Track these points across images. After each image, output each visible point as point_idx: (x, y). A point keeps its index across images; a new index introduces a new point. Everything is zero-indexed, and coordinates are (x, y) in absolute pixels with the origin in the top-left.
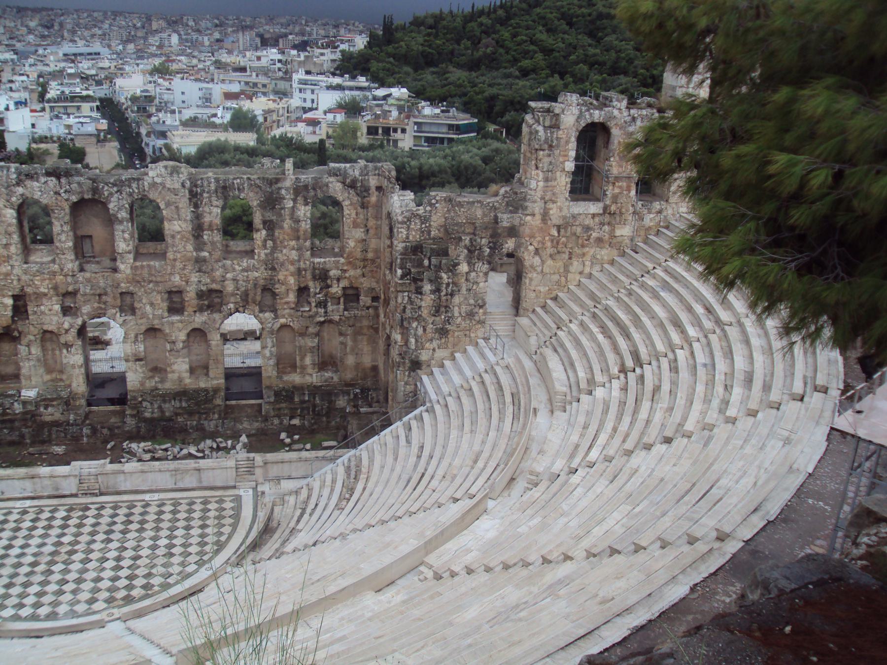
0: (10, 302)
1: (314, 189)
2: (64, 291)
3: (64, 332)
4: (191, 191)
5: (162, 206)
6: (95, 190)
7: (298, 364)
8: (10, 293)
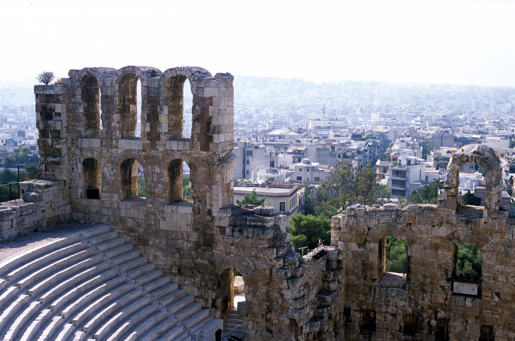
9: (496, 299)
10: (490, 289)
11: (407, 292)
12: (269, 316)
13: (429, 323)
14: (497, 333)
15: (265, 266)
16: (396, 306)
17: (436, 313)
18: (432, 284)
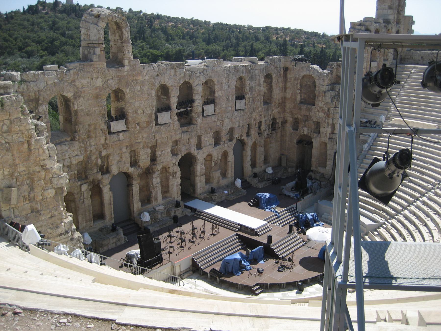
0: (149, 151)
1: (265, 70)
2: (175, 139)
3: (172, 165)
4: (227, 74)
5: (216, 83)
6: (190, 76)
7: (258, 161)
8: (150, 145)
9: (138, 128)
10: (134, 122)
11: (77, 143)
12: (32, 195)
13: (96, 164)
14: (141, 153)
15: (21, 140)
16: (70, 158)
17: (100, 152)
18: (95, 129)
